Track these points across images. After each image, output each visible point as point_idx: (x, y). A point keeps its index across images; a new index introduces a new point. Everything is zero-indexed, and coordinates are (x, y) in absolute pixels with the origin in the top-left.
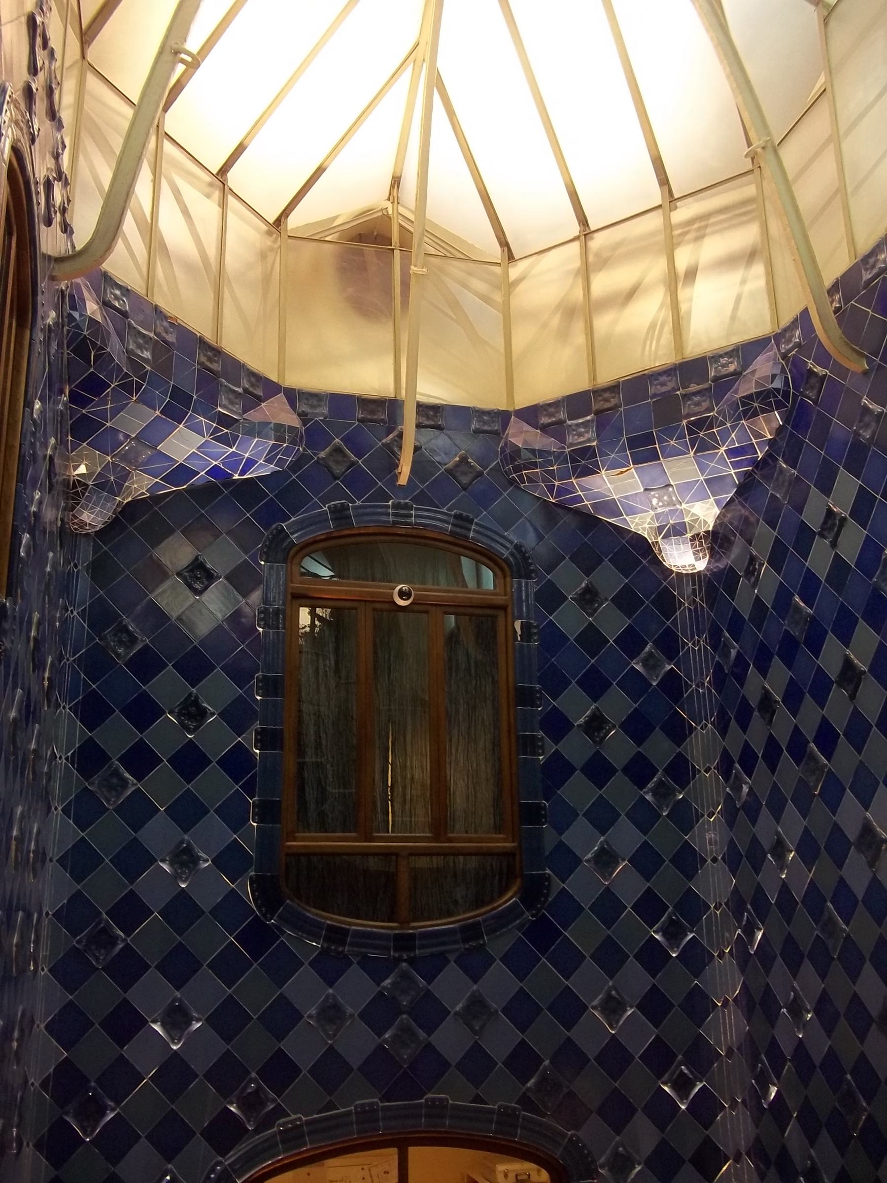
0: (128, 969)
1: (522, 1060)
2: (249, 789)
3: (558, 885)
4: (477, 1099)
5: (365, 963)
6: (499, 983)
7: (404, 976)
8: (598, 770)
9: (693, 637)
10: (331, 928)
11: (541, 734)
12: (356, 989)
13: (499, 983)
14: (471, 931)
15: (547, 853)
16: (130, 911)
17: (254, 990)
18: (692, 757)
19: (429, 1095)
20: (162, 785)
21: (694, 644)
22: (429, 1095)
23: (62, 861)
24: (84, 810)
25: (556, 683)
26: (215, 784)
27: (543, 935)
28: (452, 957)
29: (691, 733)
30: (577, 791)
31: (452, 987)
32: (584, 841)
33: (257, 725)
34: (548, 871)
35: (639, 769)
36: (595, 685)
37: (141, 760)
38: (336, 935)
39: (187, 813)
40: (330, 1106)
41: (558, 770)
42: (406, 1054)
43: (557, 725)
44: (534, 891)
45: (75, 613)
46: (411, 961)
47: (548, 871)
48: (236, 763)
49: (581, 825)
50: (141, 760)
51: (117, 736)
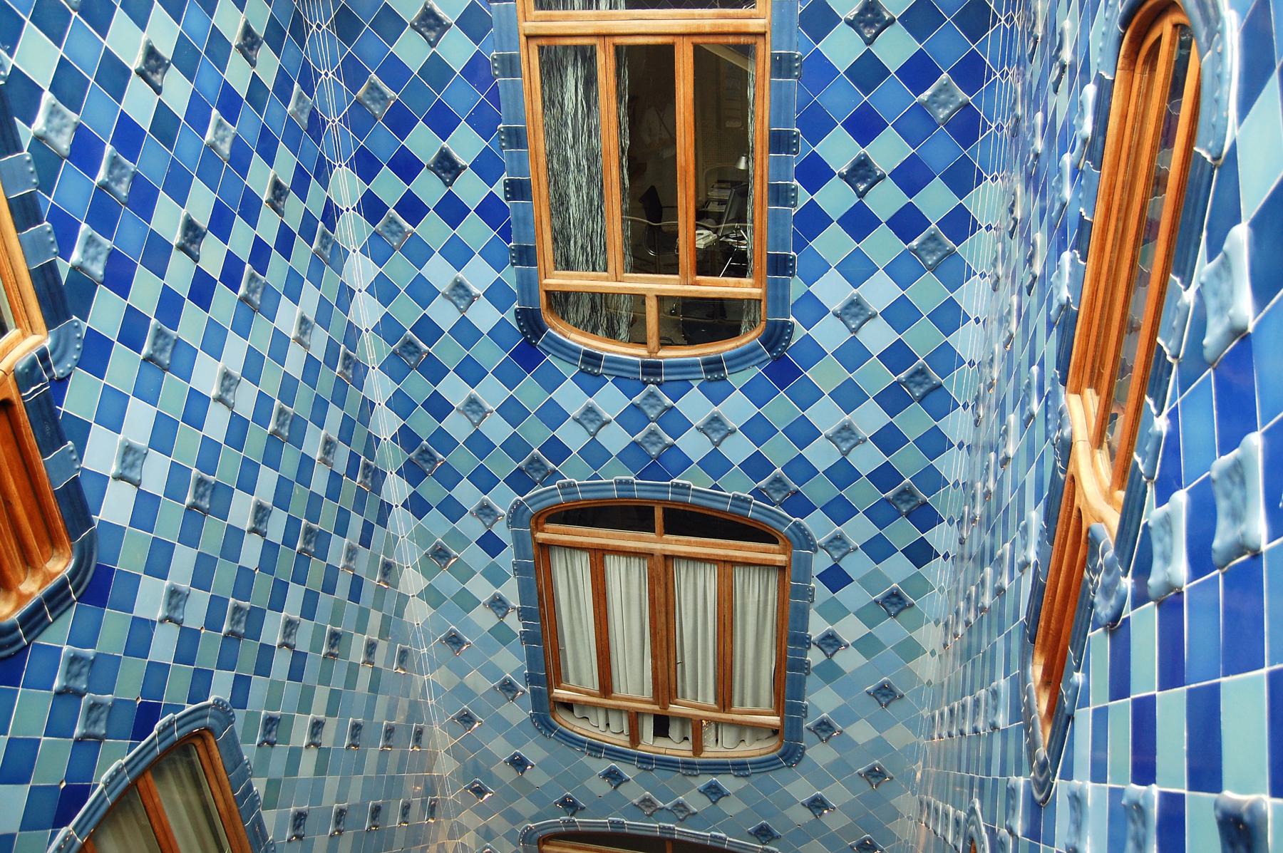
0: (435, 371)
1: (756, 466)
2: (506, 234)
3: (800, 331)
4: (715, 487)
5: (618, 380)
6: (737, 409)
7: (652, 395)
8: (859, 222)
9: (1002, 67)
10: (587, 354)
11: (795, 182)
12: (611, 400)
13: (737, 409)
14: (714, 365)
15: (793, 298)
16: (427, 329)
17: (530, 391)
18: (975, 211)
19: (675, 480)
20: (433, 229)
21: (1002, 75)
22: (675, 480)
23: (369, 290)
24: (377, 250)
25: (817, 125)
26: (475, 231)
27: (783, 369)
28: (695, 384)
29: (979, 183)
30: (833, 243)
31: (695, 405)
32: (832, 290)
33: (505, 177)
34: (792, 319)
35: (907, 223)
36: (865, 126)
37: (412, 208)
38: (592, 359)
39: (458, 254)
40: (596, 477)
41: (814, 221)
42: (654, 451)
43: (815, 173)
44: (776, 336)
45: (330, 75)
46: (659, 384)
47: (792, 319)
48: (490, 210)
49: (833, 277)
50: (412, 208)
51: (389, 187)
